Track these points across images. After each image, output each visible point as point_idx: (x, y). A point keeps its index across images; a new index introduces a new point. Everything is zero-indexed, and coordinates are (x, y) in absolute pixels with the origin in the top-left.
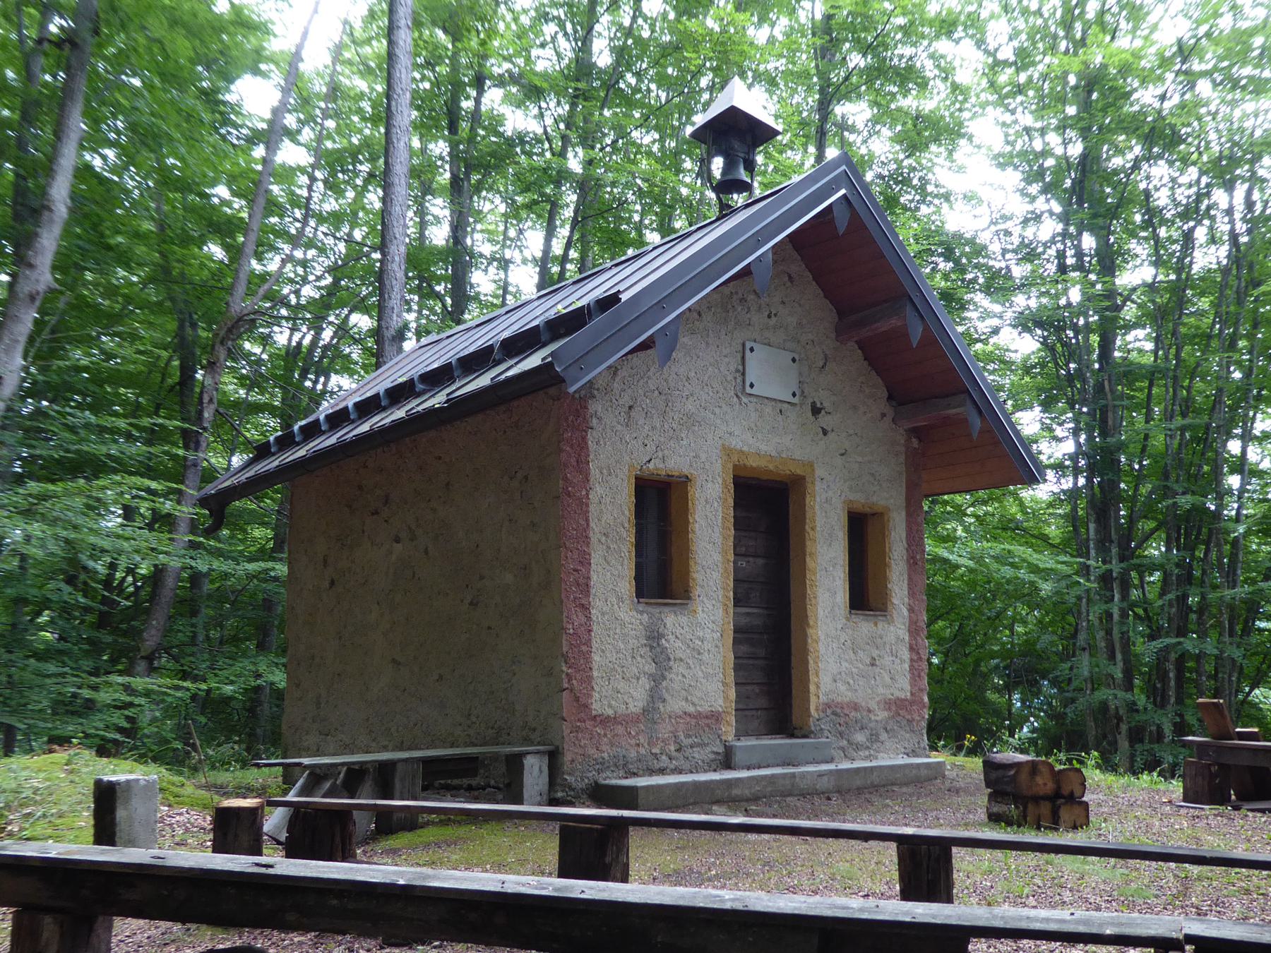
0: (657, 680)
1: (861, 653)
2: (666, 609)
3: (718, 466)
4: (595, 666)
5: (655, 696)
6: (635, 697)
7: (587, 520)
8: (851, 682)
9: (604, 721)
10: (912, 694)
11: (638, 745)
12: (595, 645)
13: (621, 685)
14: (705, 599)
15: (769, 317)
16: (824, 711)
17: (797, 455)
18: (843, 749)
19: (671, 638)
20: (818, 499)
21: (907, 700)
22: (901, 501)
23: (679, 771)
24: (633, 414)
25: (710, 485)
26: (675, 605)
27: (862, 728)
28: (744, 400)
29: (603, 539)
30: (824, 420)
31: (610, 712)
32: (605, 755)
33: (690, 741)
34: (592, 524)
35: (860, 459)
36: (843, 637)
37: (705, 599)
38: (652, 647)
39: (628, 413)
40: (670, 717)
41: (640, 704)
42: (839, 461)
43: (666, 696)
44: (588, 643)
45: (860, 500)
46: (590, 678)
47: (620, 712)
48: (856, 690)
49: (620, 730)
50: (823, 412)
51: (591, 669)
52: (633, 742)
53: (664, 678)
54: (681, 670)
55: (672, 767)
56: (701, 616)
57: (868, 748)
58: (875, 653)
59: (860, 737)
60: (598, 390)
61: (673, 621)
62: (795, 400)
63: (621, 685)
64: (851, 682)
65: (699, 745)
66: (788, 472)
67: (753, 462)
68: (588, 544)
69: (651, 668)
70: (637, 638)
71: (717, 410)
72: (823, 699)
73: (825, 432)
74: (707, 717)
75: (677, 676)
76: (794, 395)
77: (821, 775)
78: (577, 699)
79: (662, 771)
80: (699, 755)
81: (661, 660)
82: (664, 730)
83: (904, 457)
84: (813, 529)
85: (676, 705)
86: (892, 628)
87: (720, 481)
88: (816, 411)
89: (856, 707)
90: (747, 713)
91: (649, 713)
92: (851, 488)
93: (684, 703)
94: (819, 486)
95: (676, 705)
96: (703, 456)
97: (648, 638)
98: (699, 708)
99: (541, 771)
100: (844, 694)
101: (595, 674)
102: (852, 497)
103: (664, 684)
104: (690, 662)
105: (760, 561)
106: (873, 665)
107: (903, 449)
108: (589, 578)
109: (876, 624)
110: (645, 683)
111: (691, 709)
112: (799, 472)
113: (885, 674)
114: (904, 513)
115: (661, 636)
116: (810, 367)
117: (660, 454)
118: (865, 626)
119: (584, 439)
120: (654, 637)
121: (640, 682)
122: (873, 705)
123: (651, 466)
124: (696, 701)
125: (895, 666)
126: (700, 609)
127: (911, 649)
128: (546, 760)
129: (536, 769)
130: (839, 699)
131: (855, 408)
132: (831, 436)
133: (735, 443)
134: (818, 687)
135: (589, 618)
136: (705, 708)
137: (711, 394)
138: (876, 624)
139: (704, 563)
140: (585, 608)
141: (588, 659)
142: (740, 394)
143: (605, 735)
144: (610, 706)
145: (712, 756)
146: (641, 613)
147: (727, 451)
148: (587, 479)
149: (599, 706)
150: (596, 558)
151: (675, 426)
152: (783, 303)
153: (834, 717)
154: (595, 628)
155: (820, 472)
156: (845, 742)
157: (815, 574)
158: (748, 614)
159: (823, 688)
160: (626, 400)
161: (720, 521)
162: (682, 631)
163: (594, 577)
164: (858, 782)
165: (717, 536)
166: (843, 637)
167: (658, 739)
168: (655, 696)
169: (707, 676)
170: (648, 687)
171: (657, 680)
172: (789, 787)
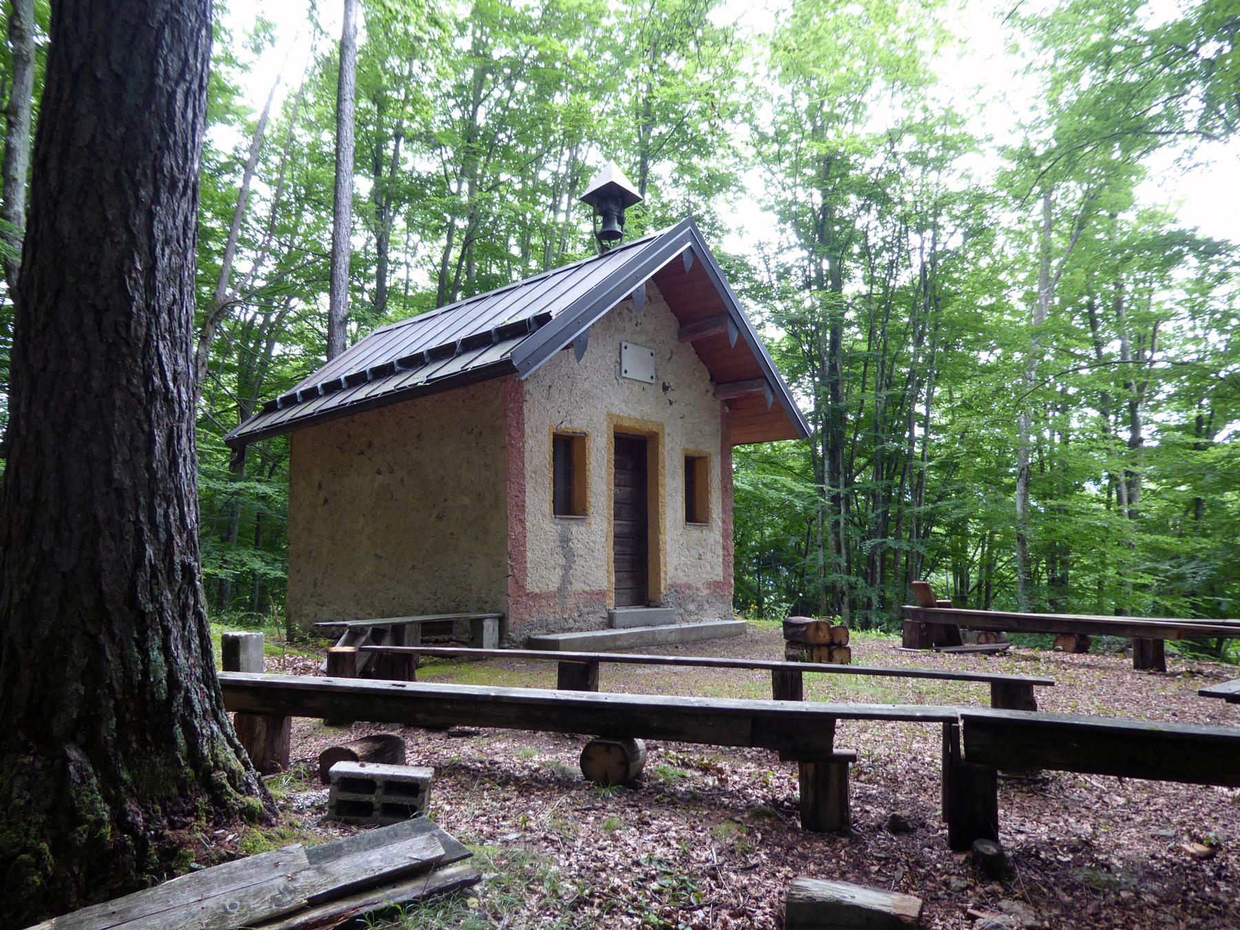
0: (567, 568)
5: (565, 580)
6: (552, 580)
9: (535, 597)
13: (544, 573)
17: (654, 418)
22: (719, 450)
30: (671, 395)
31: (537, 591)
41: (556, 586)
42: (679, 422)
44: (524, 545)
45: (692, 448)
49: (544, 602)
56: (594, 526)
58: (701, 551)
59: (692, 607)
61: (576, 530)
62: (653, 381)
63: (544, 573)
67: (626, 423)
69: (562, 561)
72: (669, 582)
73: (671, 403)
75: (579, 567)
77: (671, 632)
78: (517, 582)
79: (570, 630)
80: (593, 619)
81: (569, 556)
82: (571, 602)
85: (578, 586)
88: (665, 388)
89: (689, 587)
94: (667, 440)
95: (578, 586)
96: (595, 420)
100: (682, 579)
105: (628, 489)
110: (559, 572)
111: (587, 589)
115: (569, 540)
118: (695, 533)
120: (565, 541)
122: (700, 585)
123: (563, 426)
127: (724, 548)
128: (497, 623)
132: (674, 405)
133: (615, 411)
135: (524, 528)
136: (596, 588)
140: (522, 522)
141: (524, 556)
147: (610, 416)
149: (531, 587)
155: (667, 430)
159: (669, 575)
160: (547, 382)
163: (527, 500)
164: (694, 637)
165: (604, 473)
168: (565, 580)
169: (597, 567)
171: (567, 568)
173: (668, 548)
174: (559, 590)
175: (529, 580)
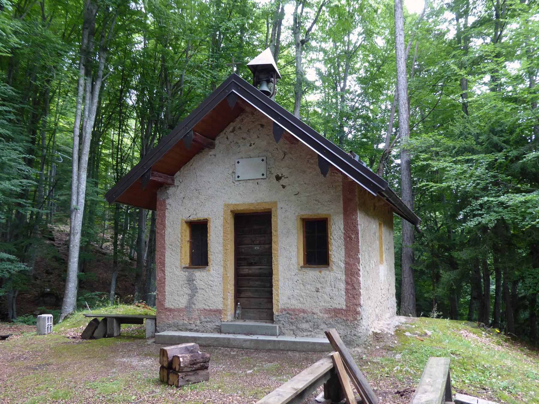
0: (192, 296)
1: (309, 287)
2: (196, 270)
3: (222, 213)
4: (166, 291)
5: (191, 302)
6: (182, 302)
7: (164, 241)
8: (301, 299)
9: (170, 310)
10: (347, 306)
11: (183, 320)
12: (166, 283)
14: (215, 266)
15: (251, 145)
16: (282, 312)
17: (267, 200)
18: (293, 330)
19: (199, 281)
20: (279, 217)
21: (342, 309)
22: (341, 209)
23: (197, 331)
24: (184, 200)
25: (217, 220)
26: (200, 268)
27: (307, 322)
28: (237, 183)
29: (170, 247)
30: (283, 181)
31: (172, 307)
32: (170, 322)
33: (206, 320)
34: (166, 242)
35: (308, 195)
36: (296, 278)
37: (215, 266)
38: (189, 284)
39: (182, 201)
40: (198, 310)
41: (184, 305)
42: (294, 198)
43: (195, 302)
44: (164, 283)
45: (308, 213)
46: (164, 295)
47: (176, 307)
48: (304, 303)
49: (176, 313)
50: (283, 178)
51: (165, 292)
52: (181, 318)
53: (195, 296)
54: (202, 293)
55: (195, 329)
56: (212, 272)
57: (311, 331)
58: (319, 286)
59: (305, 326)
60: (171, 195)
61: (199, 275)
62: (265, 177)
64: (301, 299)
65: (210, 322)
66: (262, 208)
67: (240, 208)
68: (165, 249)
69: (189, 292)
70: (183, 281)
71: (223, 191)
72: (281, 306)
73: (284, 187)
74: (214, 311)
75: (199, 296)
76: (263, 175)
77: (245, 341)
79: (191, 330)
80: (209, 325)
81: (194, 290)
82: (195, 315)
83: (341, 187)
84: (276, 231)
85: (199, 305)
86: (332, 274)
87: (222, 218)
88: (278, 178)
89: (304, 311)
90: (260, 310)
91: (188, 308)
92: (301, 209)
93: (204, 305)
94: (279, 211)
95: (199, 305)
97: (188, 281)
98: (211, 308)
99: (152, 325)
100: (295, 304)
101: (167, 293)
102: (303, 213)
103: (195, 298)
104: (207, 290)
106: (317, 291)
107: (341, 183)
108: (164, 261)
109: (320, 272)
110: (187, 297)
111: (207, 308)
112: (268, 207)
113: (325, 296)
114: (342, 216)
115: (193, 280)
116: (275, 160)
117: (195, 213)
118: (313, 274)
119: (164, 213)
120: (190, 281)
121: (185, 296)
122: (315, 311)
123: (190, 218)
124: (210, 305)
125: (334, 292)
126: (212, 269)
127: (347, 283)
128: (154, 320)
129: (150, 324)
130: (293, 307)
131: (304, 172)
134: (278, 302)
135: (165, 275)
136: (213, 307)
137: (220, 185)
138: (320, 272)
139: (214, 251)
140: (163, 271)
141: (164, 289)
142: (234, 182)
143: (170, 315)
144: (172, 305)
145: (215, 327)
146: (185, 272)
147: (227, 205)
148: (164, 226)
149: (167, 305)
150: (167, 254)
151: (202, 201)
152: (258, 137)
153: (288, 315)
154: (166, 278)
155: (279, 205)
156: (294, 327)
157: (277, 251)
158: (260, 269)
159: (281, 302)
160: (182, 195)
161: (222, 234)
162: (203, 278)
163: (166, 260)
166: (296, 278)
167: (192, 318)
168: (191, 302)
169: (214, 295)
170: (187, 299)
172: (227, 343)
173: (281, 284)
174: (186, 307)
175: (167, 301)
